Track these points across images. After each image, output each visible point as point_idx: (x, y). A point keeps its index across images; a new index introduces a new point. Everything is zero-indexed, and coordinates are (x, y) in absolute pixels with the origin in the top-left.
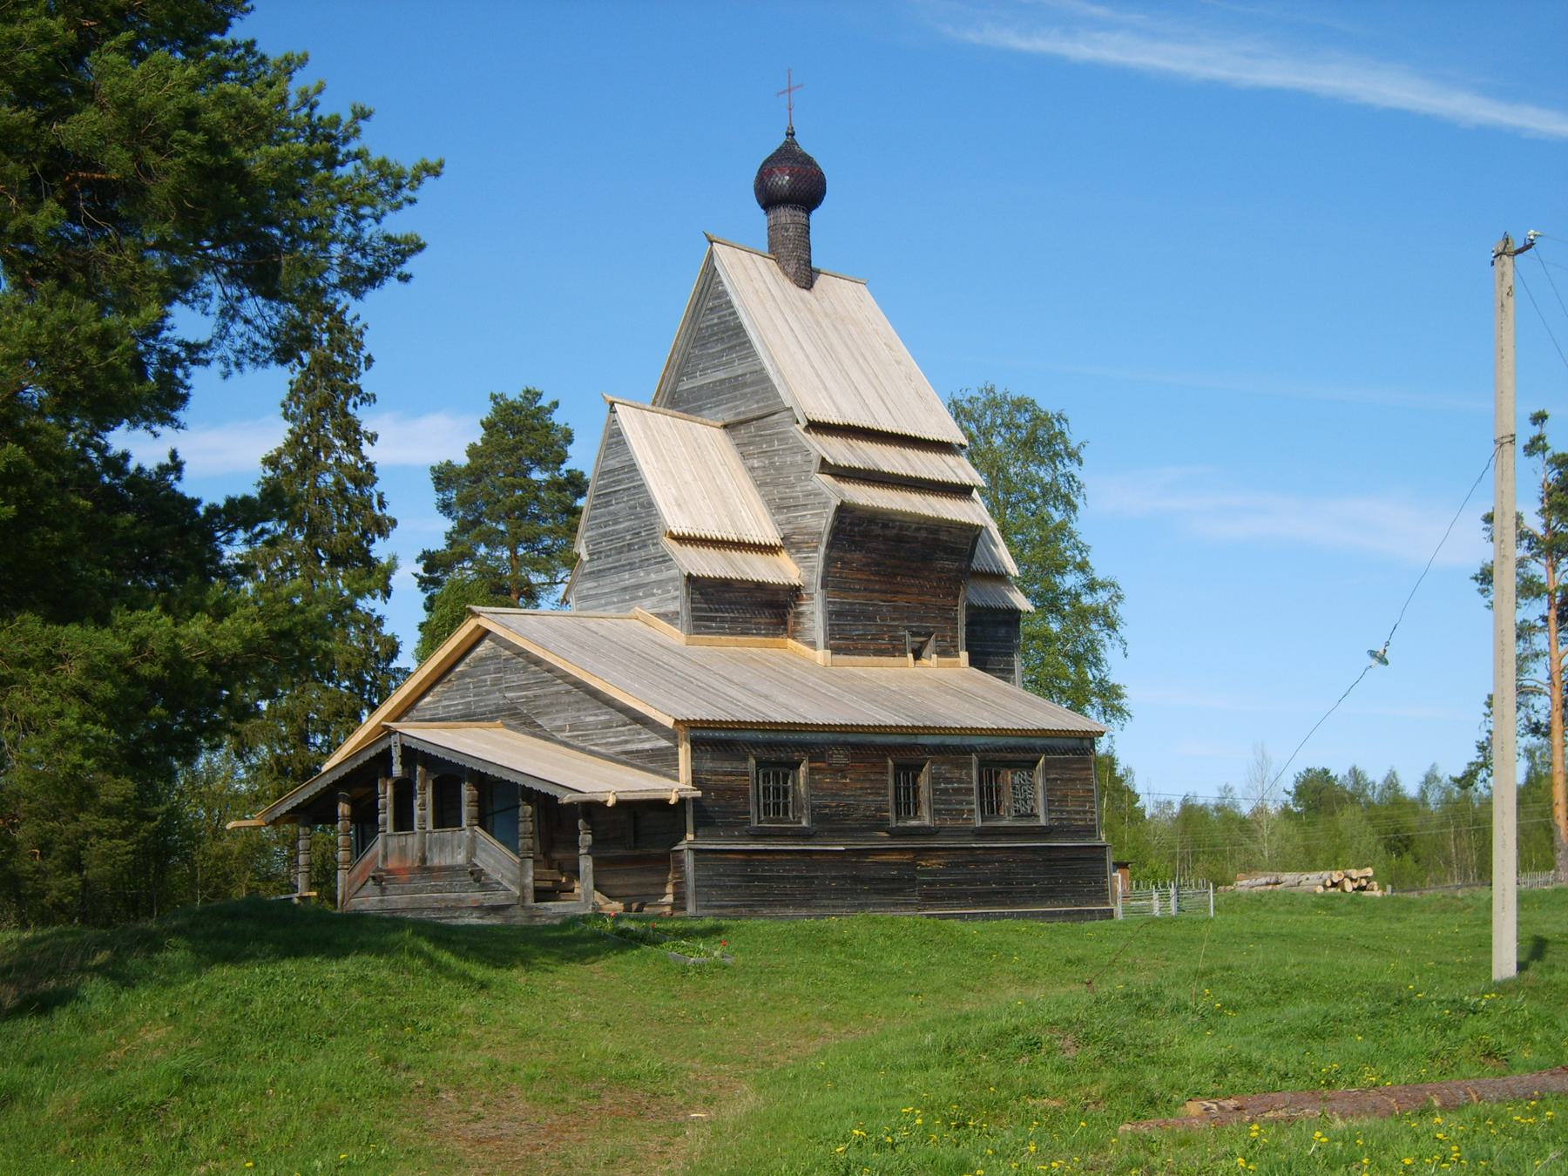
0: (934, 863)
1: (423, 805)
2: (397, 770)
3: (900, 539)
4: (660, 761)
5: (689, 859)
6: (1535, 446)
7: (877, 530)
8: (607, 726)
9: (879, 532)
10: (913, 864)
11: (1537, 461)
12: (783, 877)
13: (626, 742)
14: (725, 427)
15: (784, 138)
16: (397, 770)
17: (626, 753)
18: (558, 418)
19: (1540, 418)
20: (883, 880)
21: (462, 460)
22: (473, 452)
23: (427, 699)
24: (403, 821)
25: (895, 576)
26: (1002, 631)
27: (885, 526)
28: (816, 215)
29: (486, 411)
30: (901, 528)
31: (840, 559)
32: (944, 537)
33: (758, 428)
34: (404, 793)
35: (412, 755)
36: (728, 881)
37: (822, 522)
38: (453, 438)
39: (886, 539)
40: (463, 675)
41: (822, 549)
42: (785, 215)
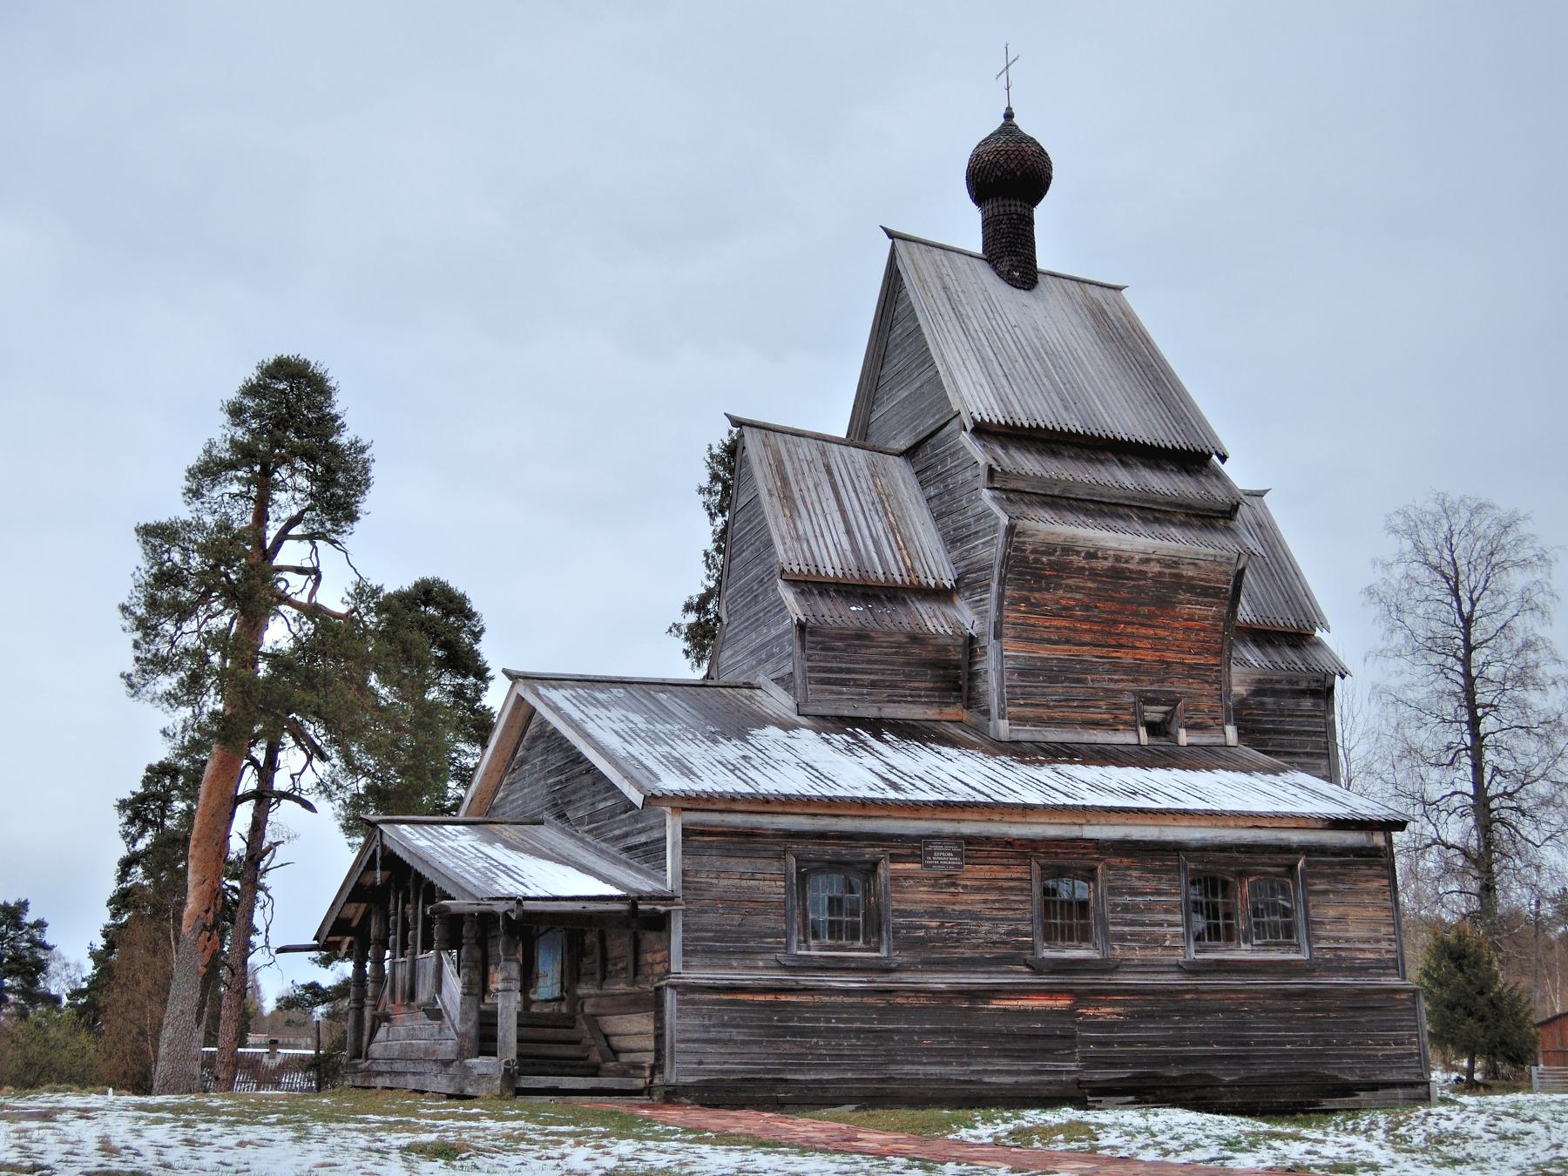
0: (1106, 1012)
7: (1079, 561)
9: (1083, 563)
10: (1070, 1013)
12: (836, 1030)
13: (626, 835)
14: (909, 454)
15: (1003, 120)
17: (628, 849)
20: (1011, 1036)
23: (500, 795)
25: (1116, 622)
26: (1307, 703)
27: (1091, 556)
30: (1118, 559)
31: (1026, 600)
32: (1189, 572)
33: (934, 447)
36: (735, 1034)
37: (991, 550)
39: (1094, 574)
41: (994, 586)
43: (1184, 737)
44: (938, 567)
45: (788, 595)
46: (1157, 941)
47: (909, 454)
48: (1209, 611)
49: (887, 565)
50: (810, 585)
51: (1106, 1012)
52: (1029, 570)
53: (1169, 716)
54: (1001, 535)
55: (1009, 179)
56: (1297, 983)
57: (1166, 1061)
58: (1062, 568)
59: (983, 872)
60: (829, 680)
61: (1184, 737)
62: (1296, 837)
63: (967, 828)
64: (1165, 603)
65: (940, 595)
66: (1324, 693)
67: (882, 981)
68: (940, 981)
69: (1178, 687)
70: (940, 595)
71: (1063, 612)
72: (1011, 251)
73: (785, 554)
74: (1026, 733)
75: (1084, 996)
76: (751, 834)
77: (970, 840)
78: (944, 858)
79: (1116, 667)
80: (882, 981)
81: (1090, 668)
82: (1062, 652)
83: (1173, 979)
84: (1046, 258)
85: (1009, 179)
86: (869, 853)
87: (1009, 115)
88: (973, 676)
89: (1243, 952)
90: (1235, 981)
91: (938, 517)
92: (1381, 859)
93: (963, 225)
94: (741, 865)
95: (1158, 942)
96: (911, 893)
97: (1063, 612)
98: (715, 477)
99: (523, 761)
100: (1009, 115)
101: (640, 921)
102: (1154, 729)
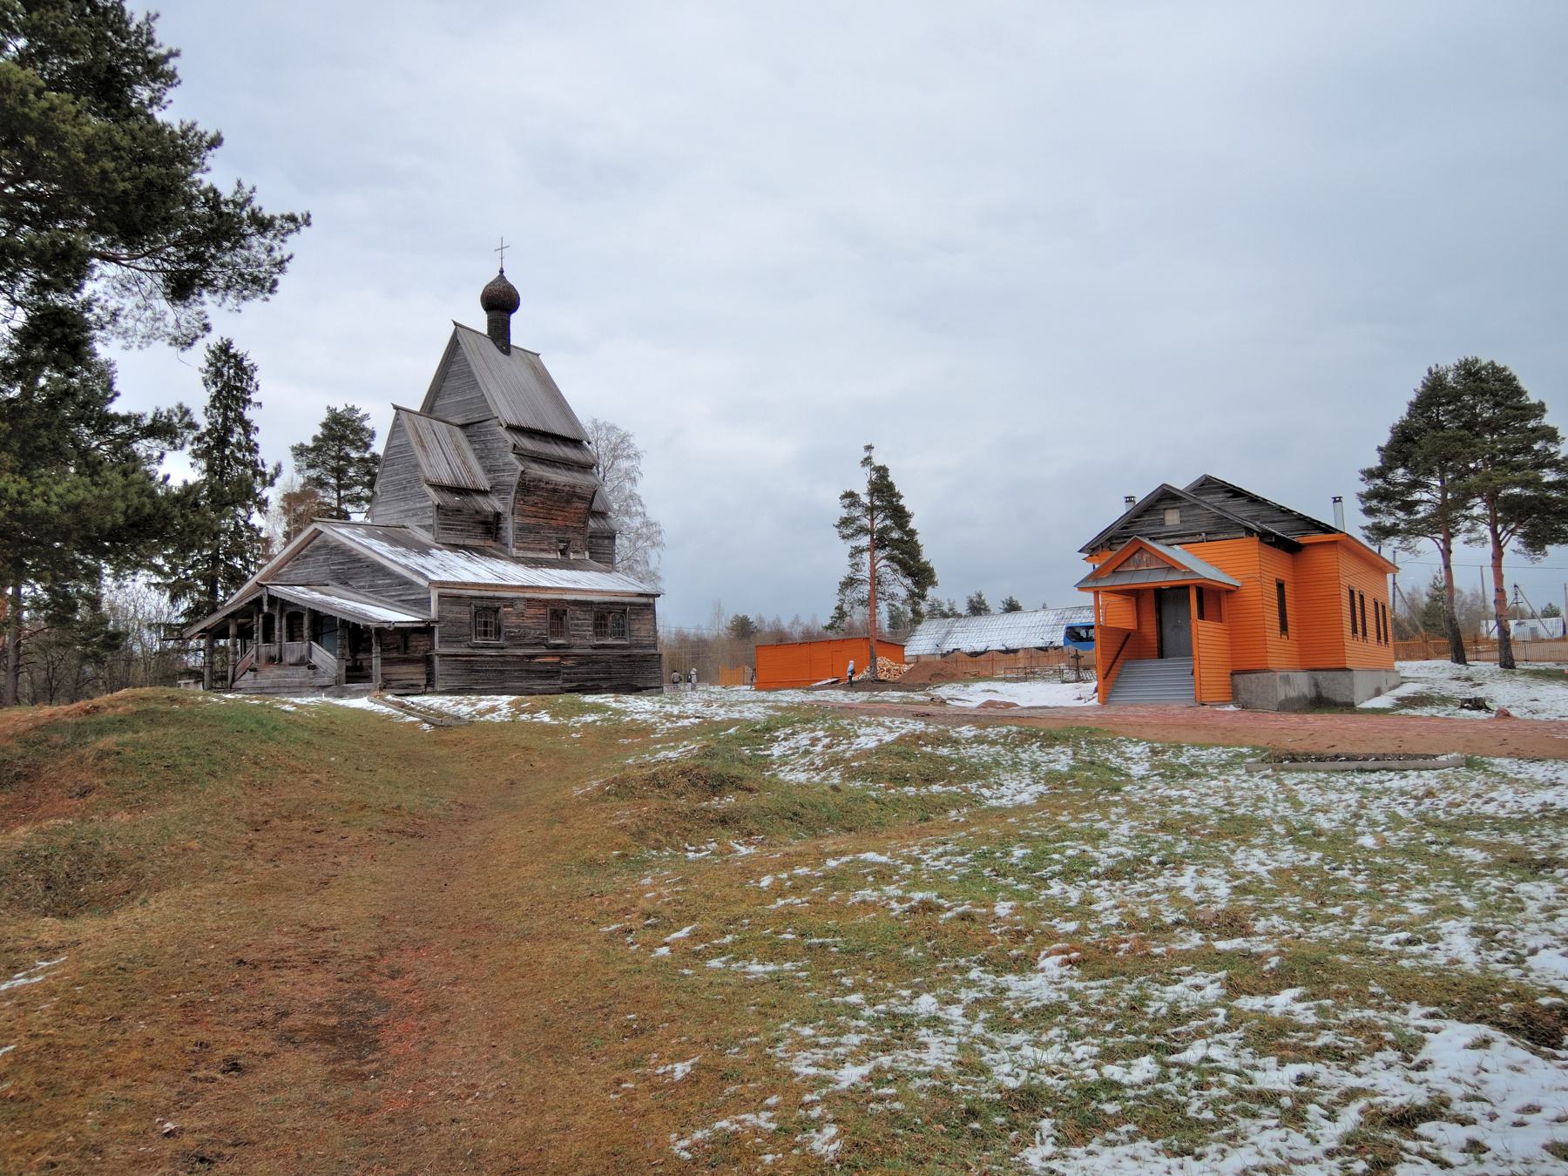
0: (569, 663)
1: (280, 625)
2: (266, 608)
3: (555, 491)
4: (423, 604)
5: (437, 659)
6: (867, 461)
8: (390, 585)
11: (868, 469)
14: (463, 427)
16: (266, 608)
18: (367, 424)
19: (869, 448)
21: (310, 444)
22: (316, 439)
24: (268, 638)
28: (514, 317)
29: (324, 416)
34: (269, 620)
35: (273, 600)
38: (309, 432)
40: (306, 556)
42: (496, 313)
43: (572, 556)
44: (484, 484)
45: (430, 491)
46: (584, 637)
47: (463, 427)
48: (582, 506)
49: (465, 481)
50: (439, 487)
51: (569, 663)
52: (526, 487)
53: (566, 548)
54: (518, 475)
55: (501, 302)
56: (625, 652)
57: (587, 680)
58: (536, 487)
59: (532, 611)
60: (447, 528)
61: (572, 556)
62: (627, 600)
63: (528, 595)
64: (568, 502)
65: (484, 493)
66: (612, 537)
67: (501, 652)
68: (519, 652)
69: (570, 536)
70: (484, 493)
71: (535, 505)
72: (500, 333)
73: (428, 473)
74: (521, 554)
75: (563, 657)
76: (459, 597)
77: (528, 600)
78: (520, 606)
79: (550, 527)
80: (501, 652)
81: (542, 527)
82: (533, 521)
83: (590, 651)
84: (515, 340)
85: (501, 302)
86: (497, 604)
87: (502, 272)
88: (498, 529)
89: (609, 641)
90: (607, 651)
91: (480, 458)
92: (650, 607)
93: (479, 320)
94: (456, 609)
95: (583, 638)
96: (510, 619)
97: (535, 505)
98: (211, 365)
99: (306, 556)
100: (502, 272)
101: (426, 630)
102: (563, 552)
